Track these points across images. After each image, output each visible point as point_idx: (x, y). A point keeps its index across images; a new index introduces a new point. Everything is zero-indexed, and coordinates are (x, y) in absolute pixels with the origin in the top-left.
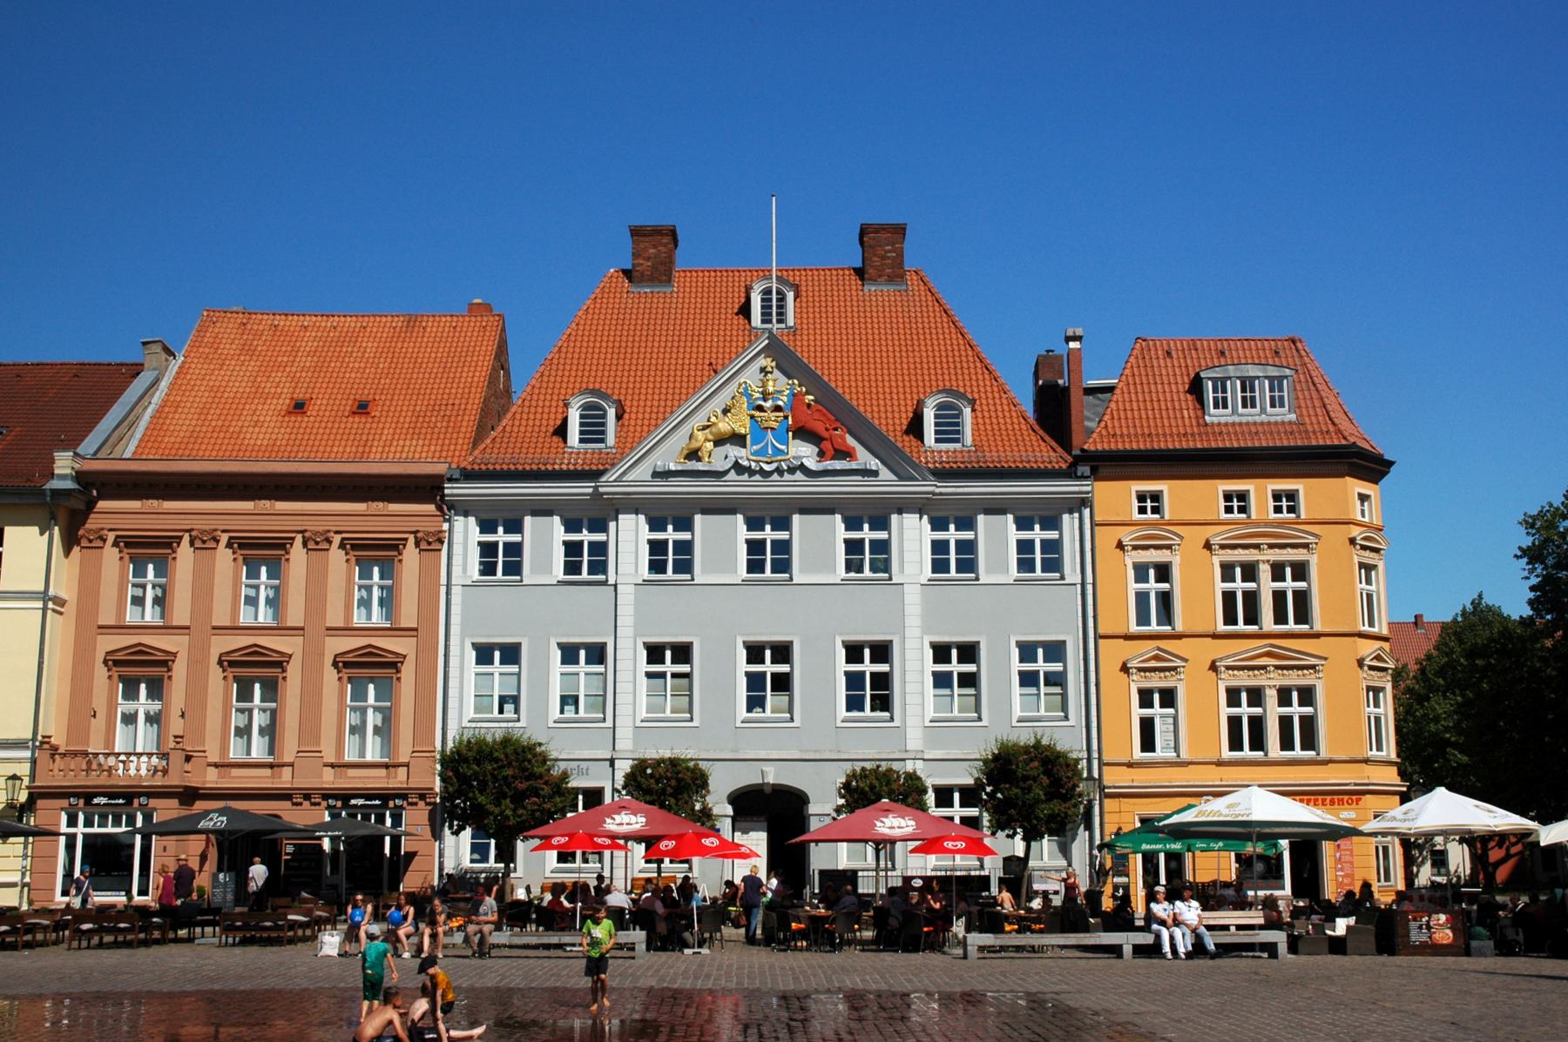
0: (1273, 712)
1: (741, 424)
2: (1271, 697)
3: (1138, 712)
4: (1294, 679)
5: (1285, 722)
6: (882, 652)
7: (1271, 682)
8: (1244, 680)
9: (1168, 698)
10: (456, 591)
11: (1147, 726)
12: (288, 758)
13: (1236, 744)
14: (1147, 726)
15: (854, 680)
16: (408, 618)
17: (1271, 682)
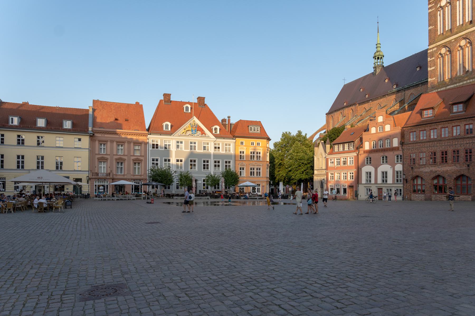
0: (255, 171)
1: (190, 129)
2: (255, 169)
3: (239, 171)
4: (258, 167)
5: (257, 172)
6: (208, 162)
7: (256, 167)
8: (252, 167)
9: (243, 169)
10: (149, 151)
11: (241, 172)
12: (126, 174)
13: (251, 175)
14: (241, 172)
15: (204, 165)
16: (143, 155)
17: (256, 167)
